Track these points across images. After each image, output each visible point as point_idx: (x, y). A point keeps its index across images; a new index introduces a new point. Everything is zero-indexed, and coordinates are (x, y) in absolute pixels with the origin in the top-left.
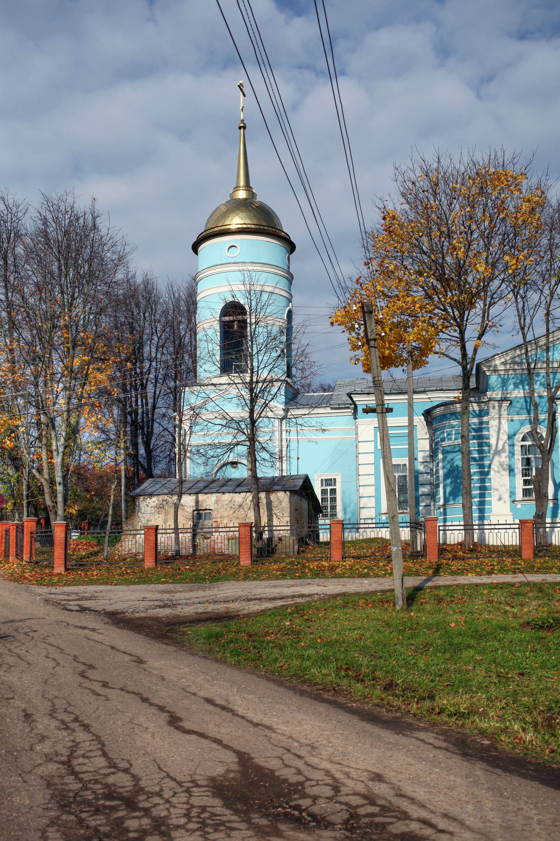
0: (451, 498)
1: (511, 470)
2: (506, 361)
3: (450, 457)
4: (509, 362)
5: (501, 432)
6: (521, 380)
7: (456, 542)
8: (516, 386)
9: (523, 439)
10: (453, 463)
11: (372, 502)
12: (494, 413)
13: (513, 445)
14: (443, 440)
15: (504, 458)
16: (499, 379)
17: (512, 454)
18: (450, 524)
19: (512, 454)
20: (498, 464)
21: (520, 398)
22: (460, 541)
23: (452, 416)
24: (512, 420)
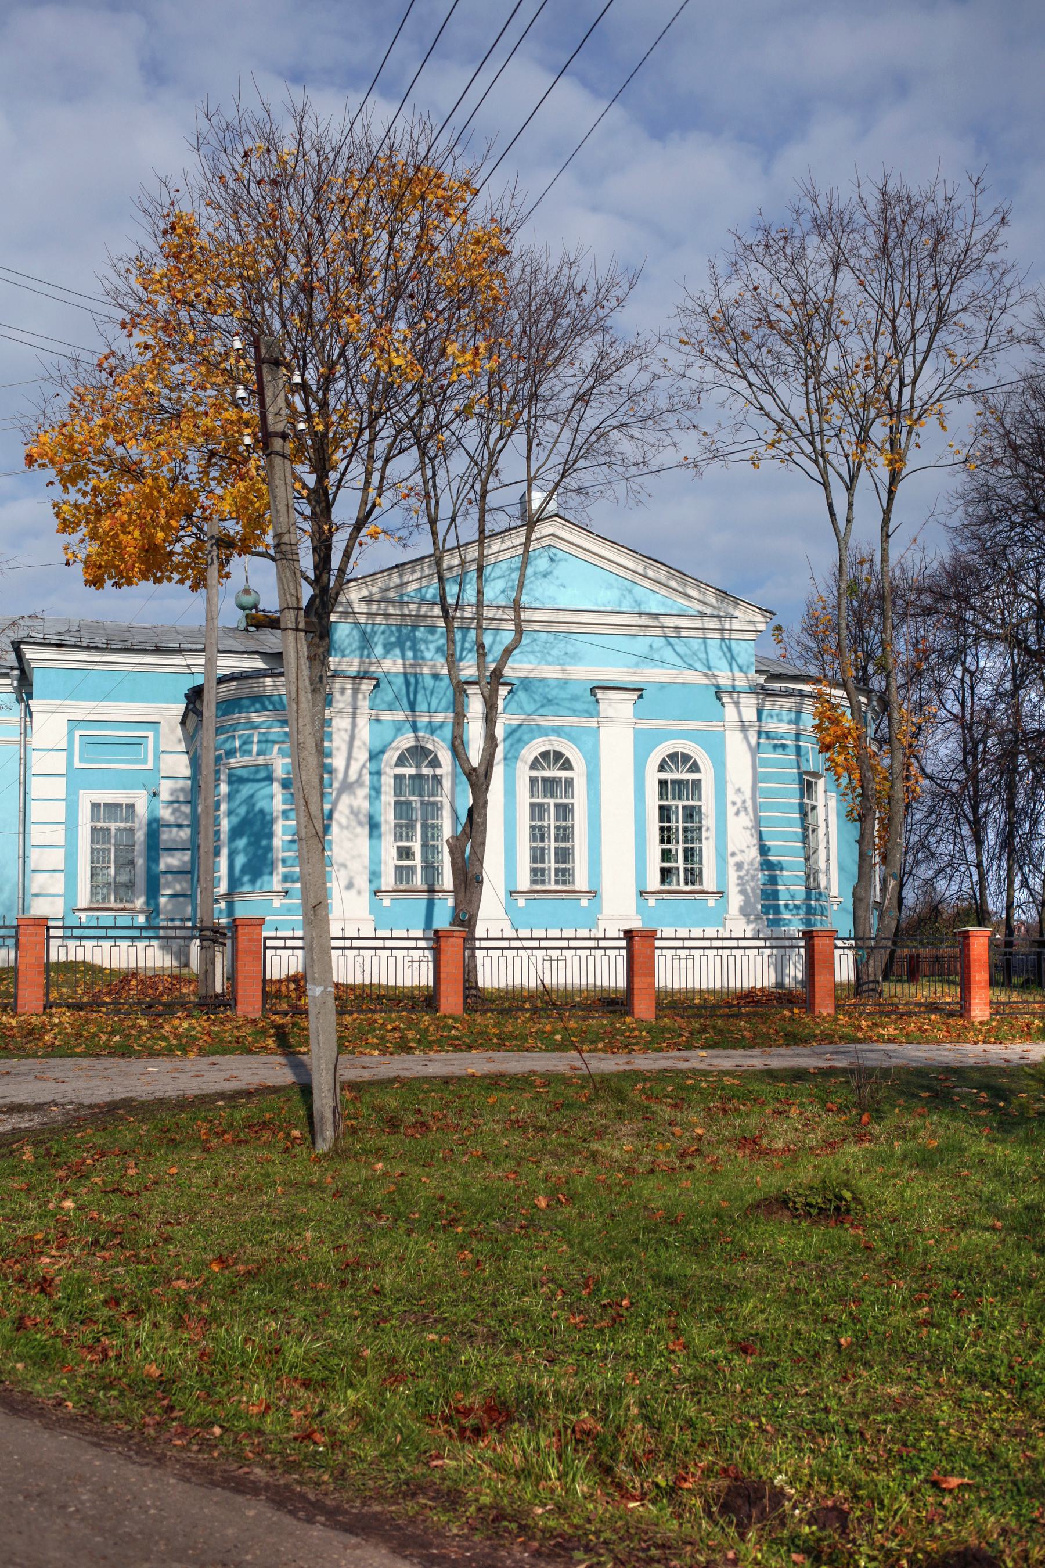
0: (246, 878)
1: (374, 826)
2: (371, 594)
3: (246, 790)
4: (376, 597)
5: (357, 743)
6: (398, 638)
7: (283, 976)
8: (388, 648)
9: (401, 761)
10: (254, 805)
11: (57, 883)
12: (342, 701)
13: (379, 773)
14: (231, 753)
15: (360, 799)
16: (355, 632)
17: (376, 791)
18: (272, 934)
19: (376, 791)
20: (347, 811)
21: (396, 674)
22: (291, 973)
23: (253, 704)
24: (378, 720)
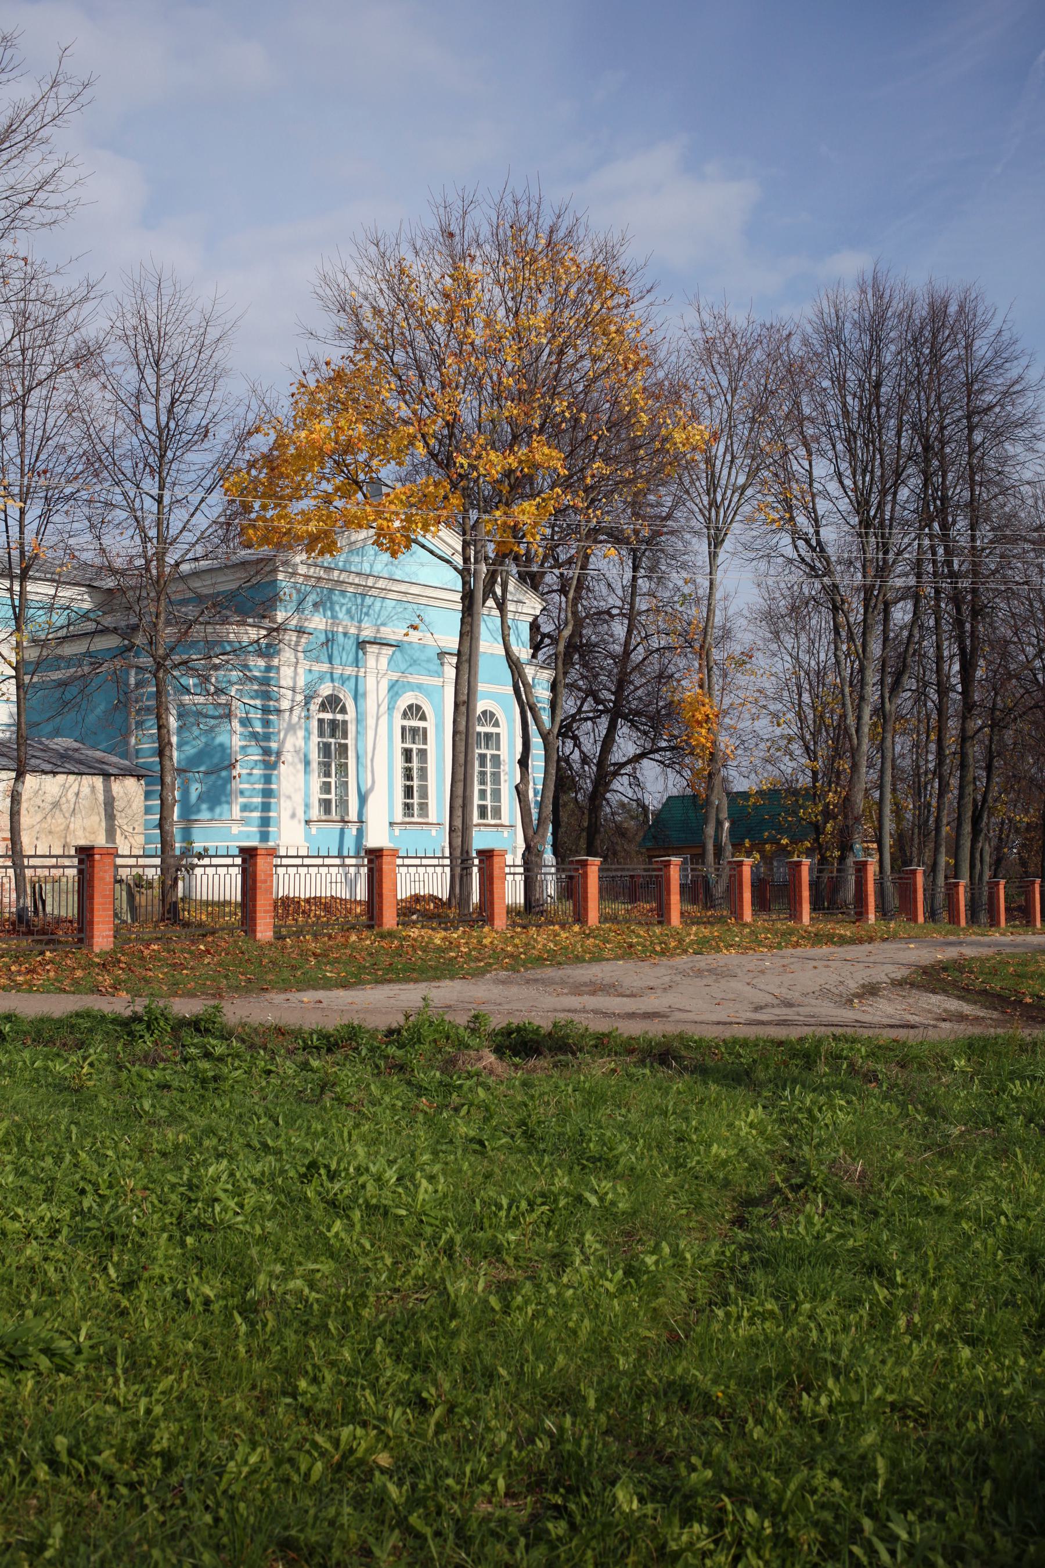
1: (307, 763)
